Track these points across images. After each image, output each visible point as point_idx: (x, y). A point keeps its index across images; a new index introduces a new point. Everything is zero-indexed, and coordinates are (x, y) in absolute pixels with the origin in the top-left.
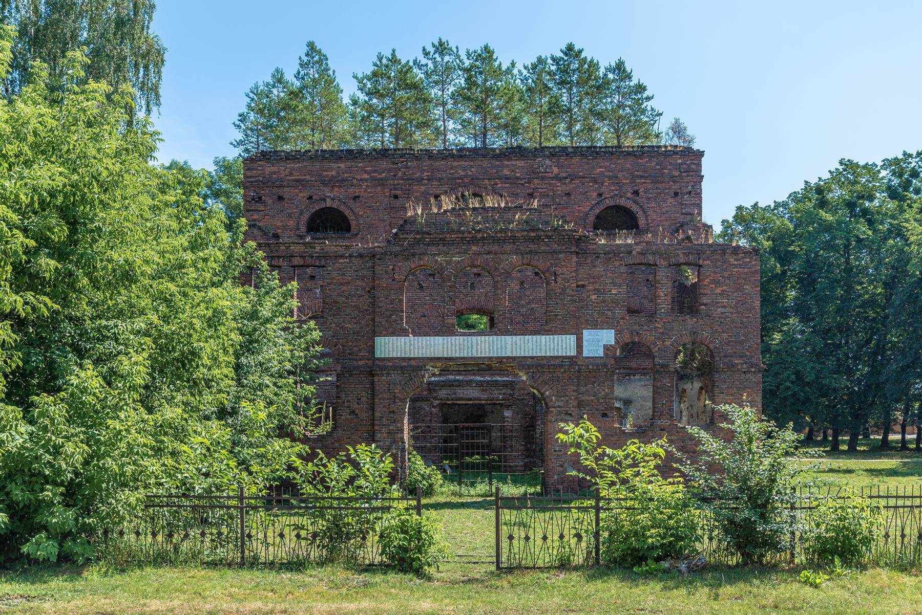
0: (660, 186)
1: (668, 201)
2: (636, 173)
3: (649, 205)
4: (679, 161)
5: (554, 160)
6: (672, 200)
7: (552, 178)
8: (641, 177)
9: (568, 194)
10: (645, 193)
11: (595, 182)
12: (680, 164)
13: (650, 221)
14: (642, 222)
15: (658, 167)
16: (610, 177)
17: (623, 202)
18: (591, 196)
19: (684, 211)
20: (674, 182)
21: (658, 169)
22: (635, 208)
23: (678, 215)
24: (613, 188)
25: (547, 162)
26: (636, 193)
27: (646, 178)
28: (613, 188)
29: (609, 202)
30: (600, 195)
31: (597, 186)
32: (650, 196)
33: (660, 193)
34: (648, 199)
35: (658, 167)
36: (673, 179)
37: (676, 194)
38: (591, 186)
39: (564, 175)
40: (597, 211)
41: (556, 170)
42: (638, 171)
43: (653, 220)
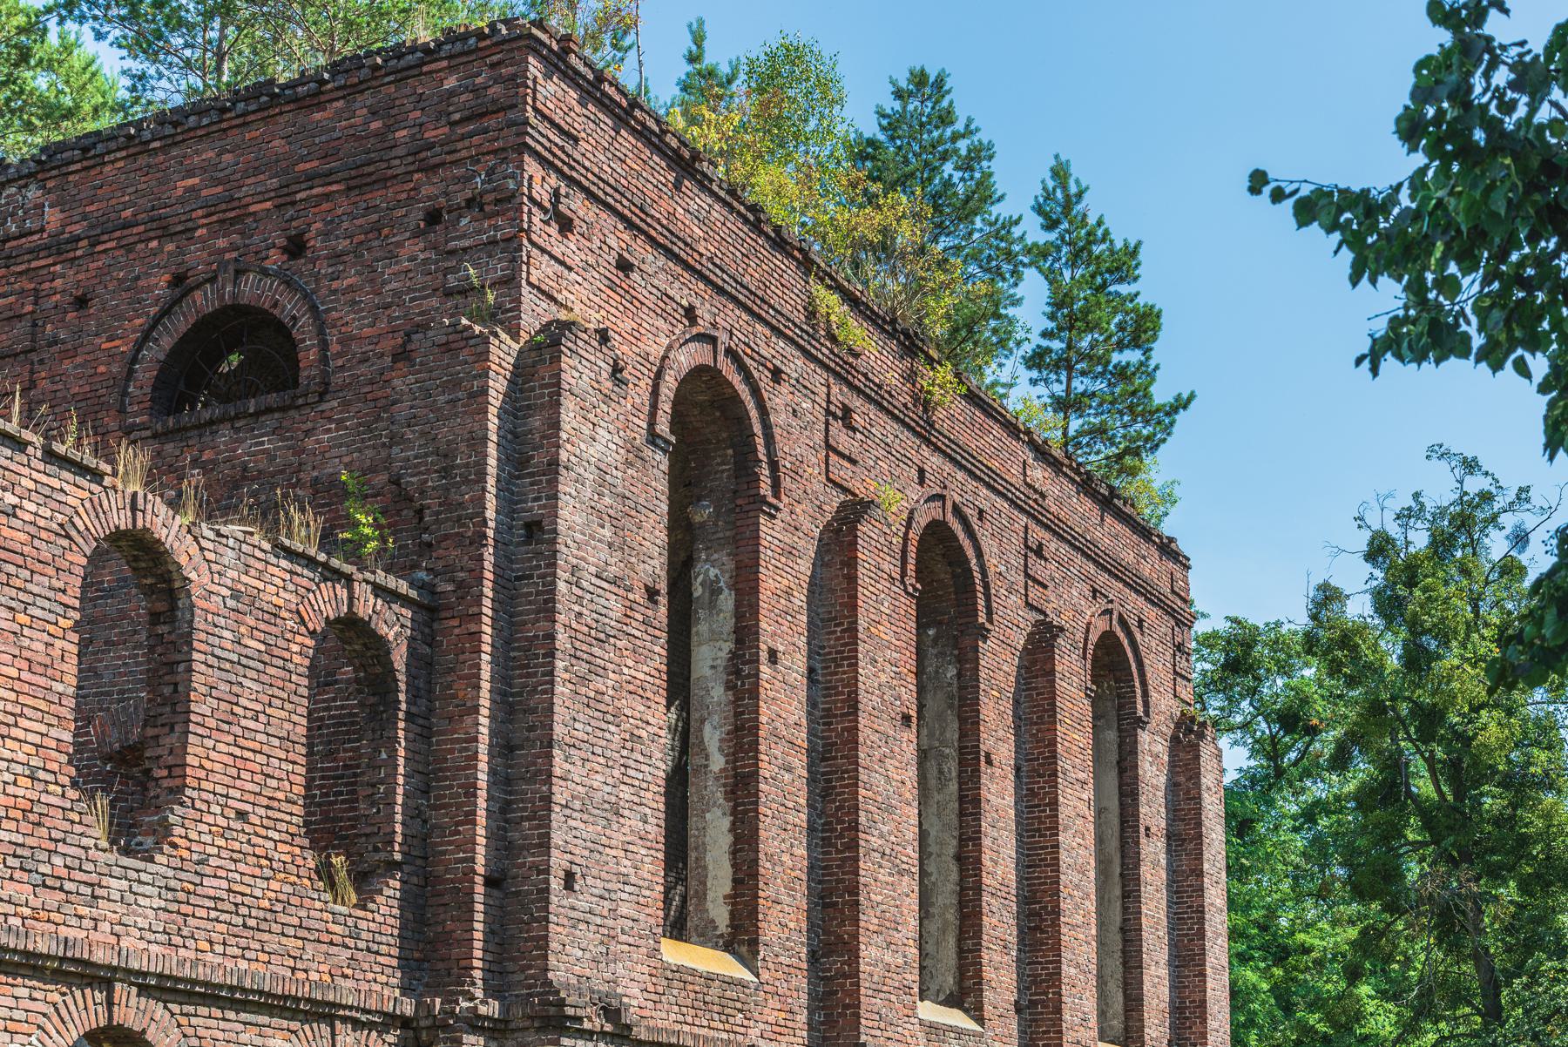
0: (378, 197)
1: (404, 253)
2: (301, 166)
3: (335, 285)
4: (451, 82)
5: (50, 184)
6: (414, 248)
7: (35, 252)
8: (311, 178)
9: (81, 302)
10: (326, 234)
11: (165, 233)
12: (452, 93)
13: (335, 348)
14: (309, 354)
15: (375, 125)
16: (210, 207)
17: (252, 289)
18: (150, 289)
19: (452, 281)
20: (431, 169)
21: (376, 134)
22: (289, 306)
23: (434, 302)
24: (222, 243)
25: (33, 193)
26: (296, 247)
27: (326, 177)
28: (222, 243)
29: (203, 301)
30: (178, 280)
31: (170, 247)
32: (343, 244)
33: (376, 228)
34: (336, 257)
35: (375, 125)
36: (424, 159)
37: (433, 217)
38: (154, 253)
39: (77, 229)
40: (167, 342)
41: (53, 217)
42: (302, 159)
43: (345, 341)
